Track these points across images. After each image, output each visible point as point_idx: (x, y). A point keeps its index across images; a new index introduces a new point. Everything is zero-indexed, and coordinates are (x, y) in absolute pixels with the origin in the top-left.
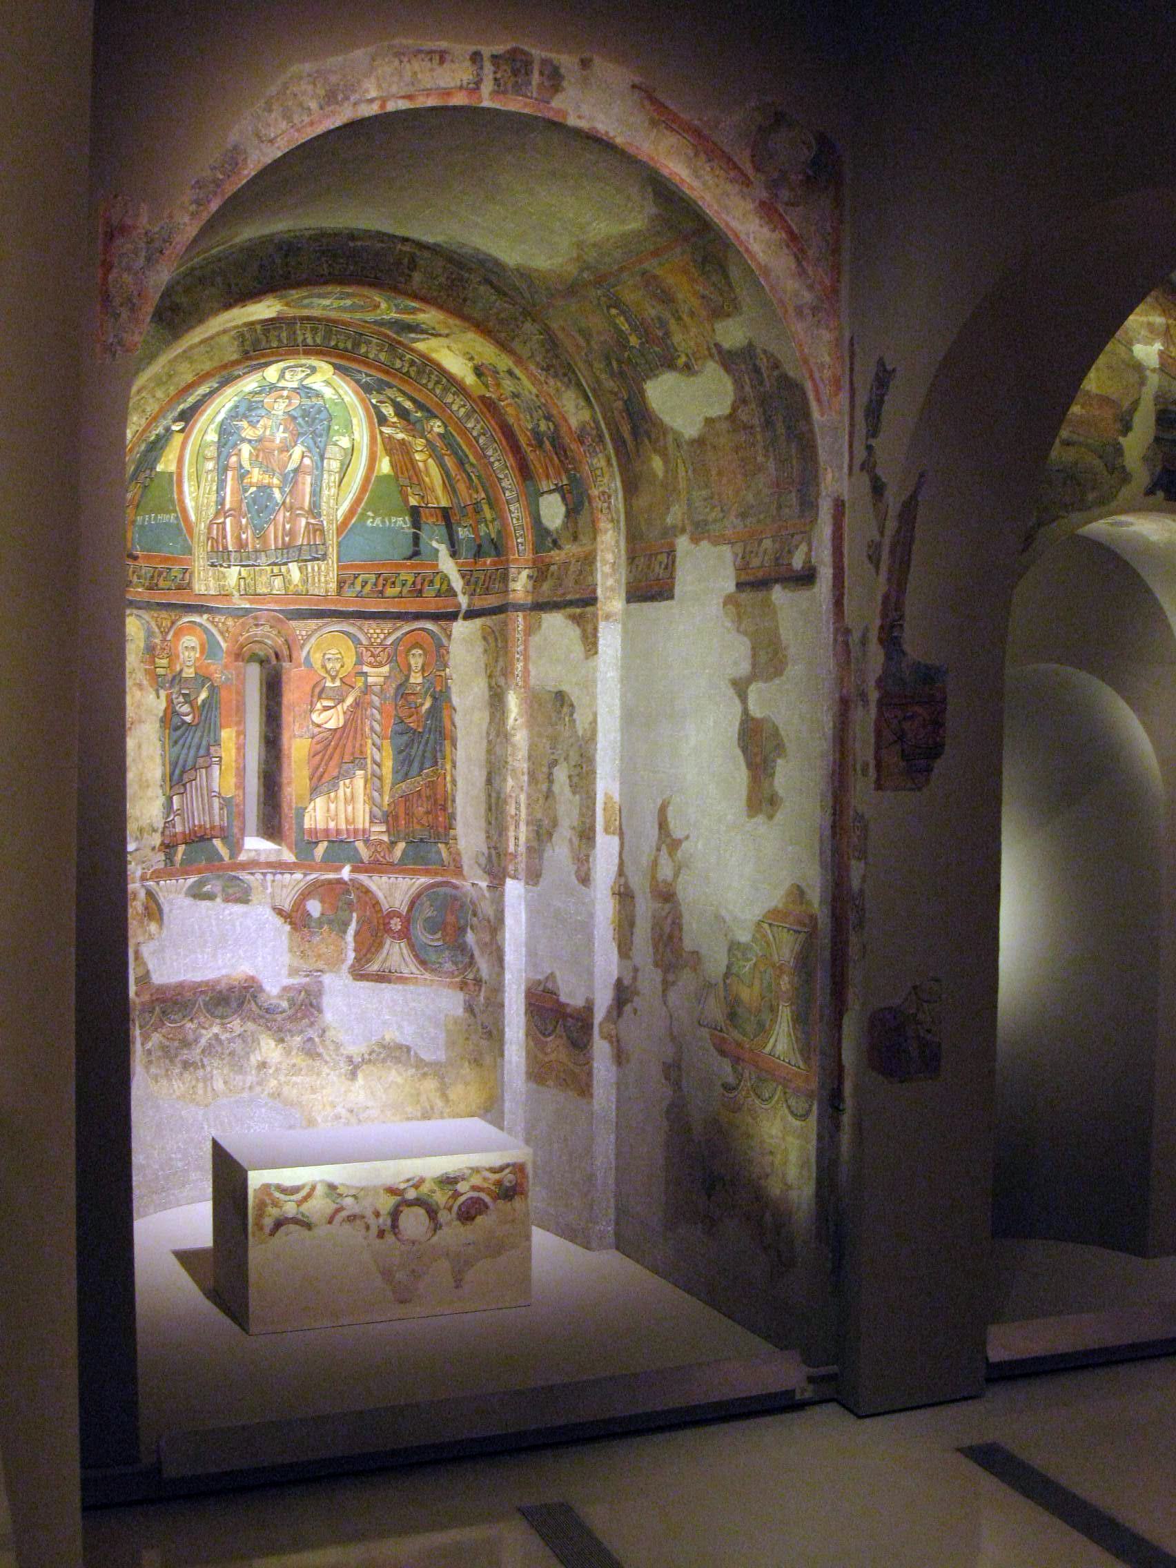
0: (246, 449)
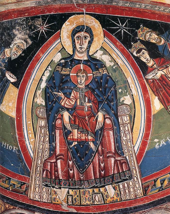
0: (66, 115)
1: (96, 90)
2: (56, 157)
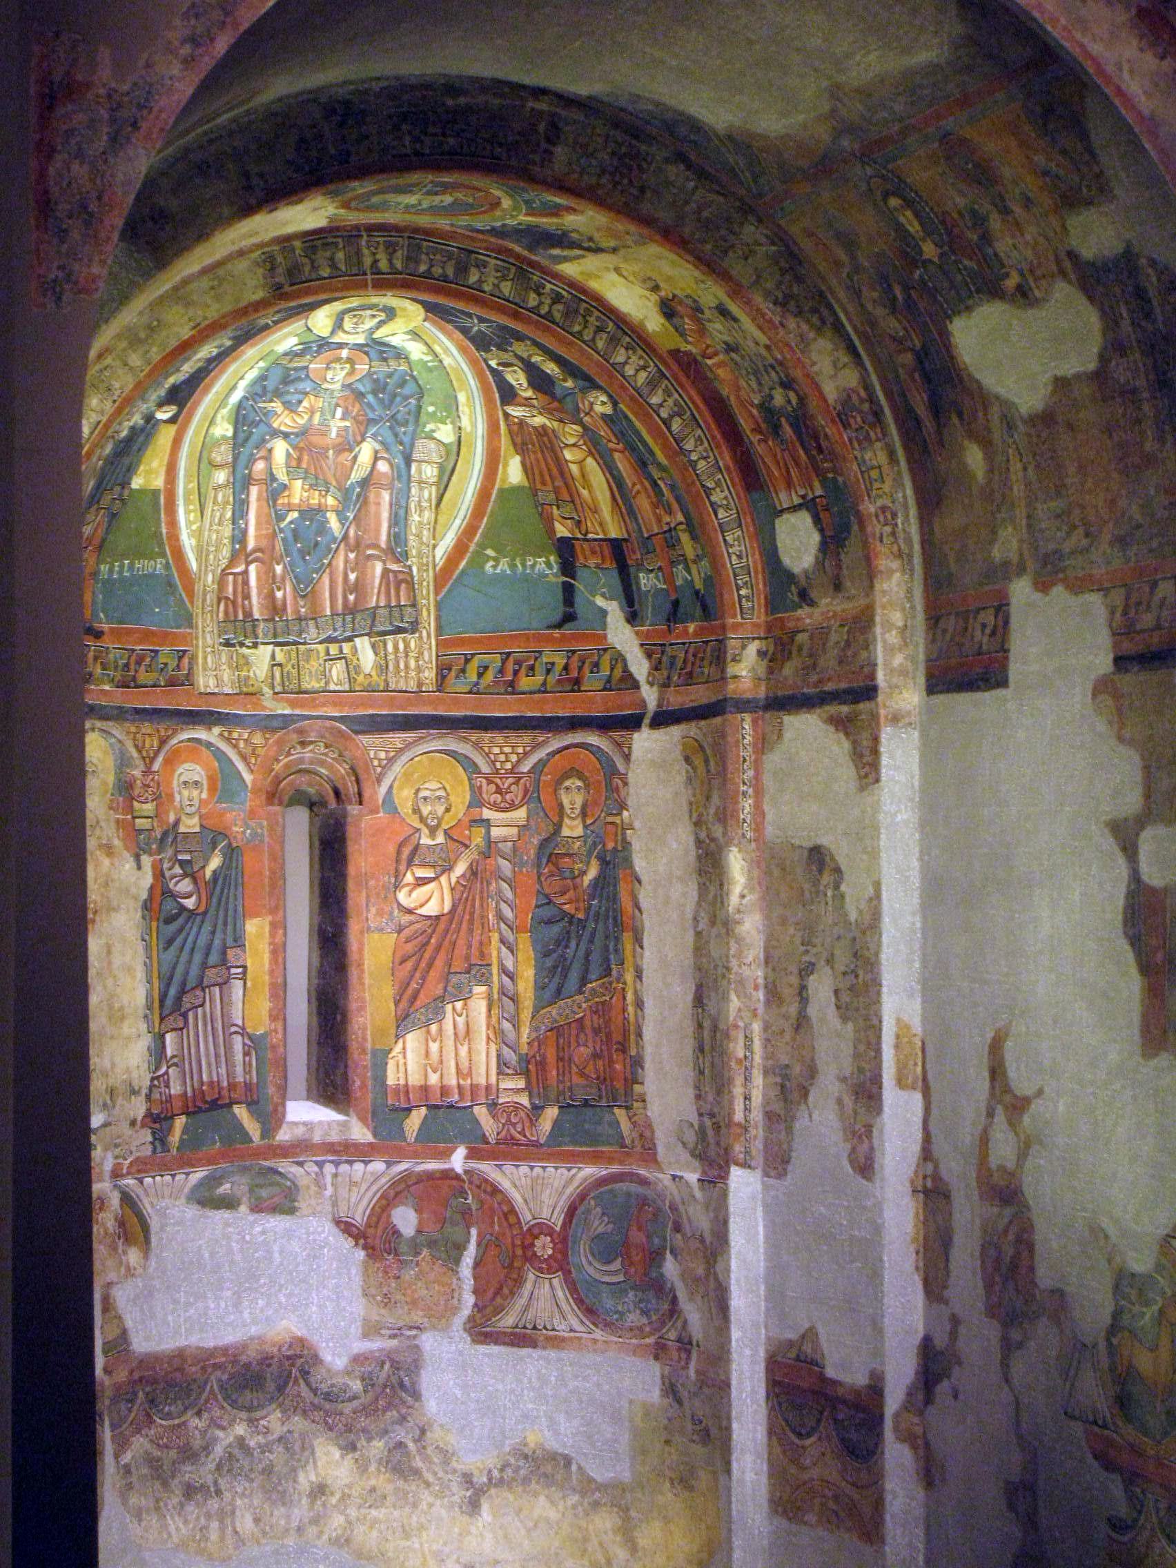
0: (280, 449)
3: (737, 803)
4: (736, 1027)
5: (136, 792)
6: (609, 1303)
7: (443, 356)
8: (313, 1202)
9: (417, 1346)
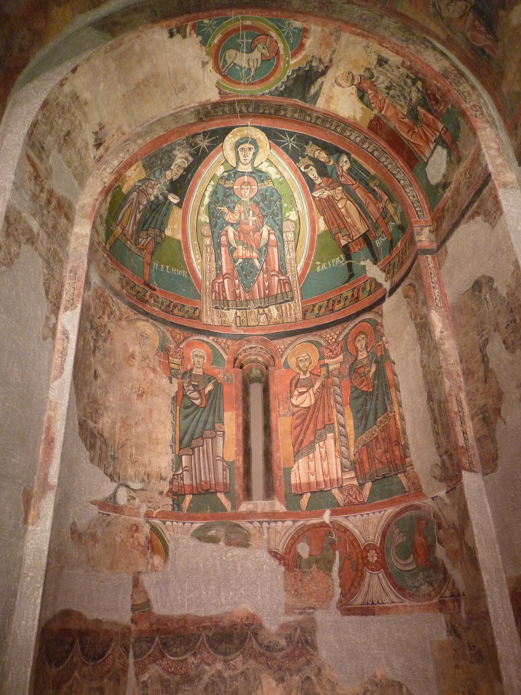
0: (231, 231)
1: (261, 204)
2: (223, 276)
3: (431, 291)
4: (452, 395)
5: (171, 353)
6: (410, 583)
7: (283, 173)
8: (258, 542)
9: (313, 619)
